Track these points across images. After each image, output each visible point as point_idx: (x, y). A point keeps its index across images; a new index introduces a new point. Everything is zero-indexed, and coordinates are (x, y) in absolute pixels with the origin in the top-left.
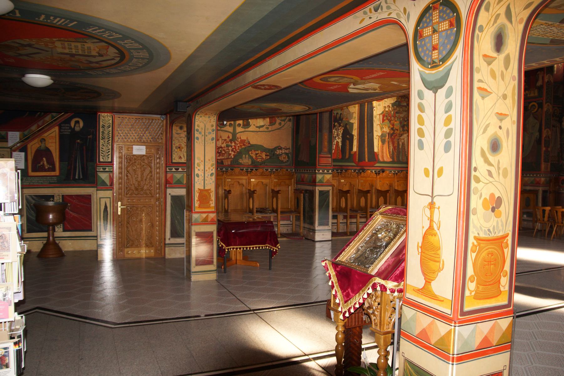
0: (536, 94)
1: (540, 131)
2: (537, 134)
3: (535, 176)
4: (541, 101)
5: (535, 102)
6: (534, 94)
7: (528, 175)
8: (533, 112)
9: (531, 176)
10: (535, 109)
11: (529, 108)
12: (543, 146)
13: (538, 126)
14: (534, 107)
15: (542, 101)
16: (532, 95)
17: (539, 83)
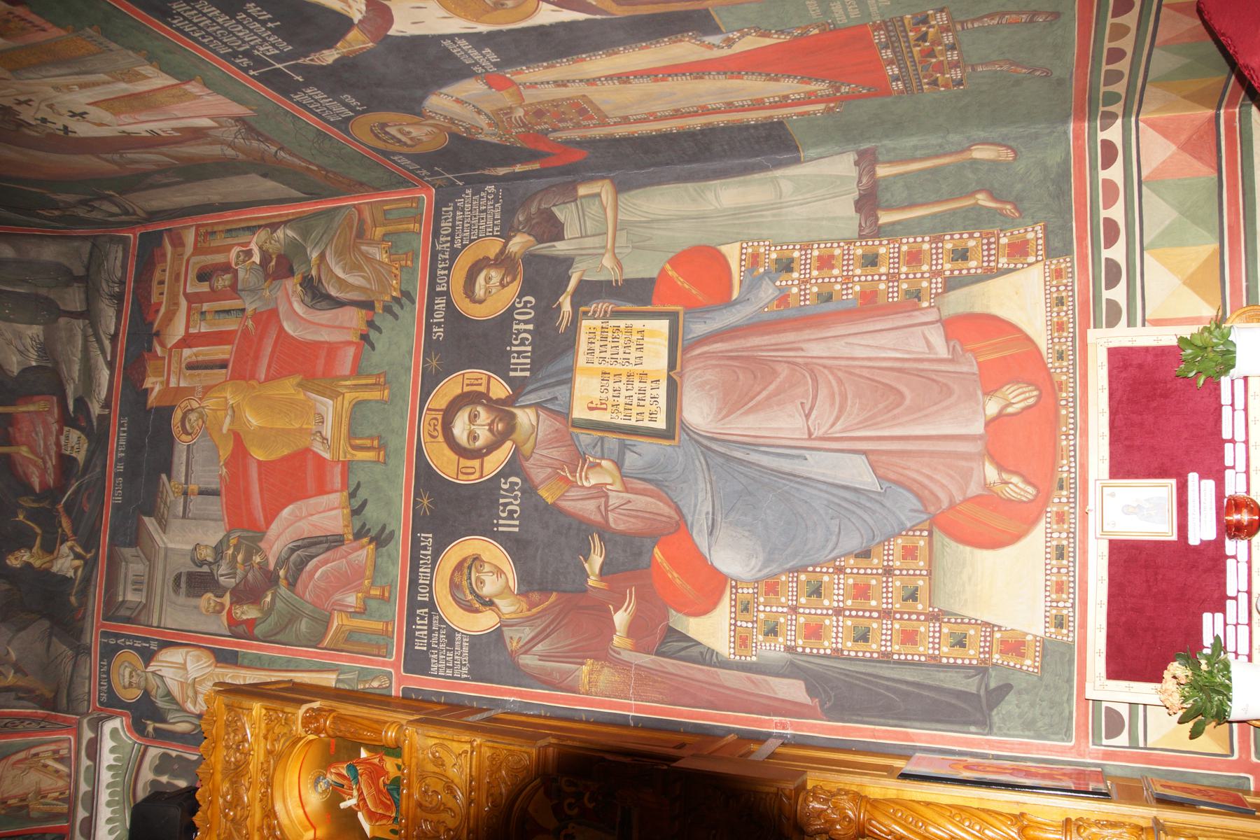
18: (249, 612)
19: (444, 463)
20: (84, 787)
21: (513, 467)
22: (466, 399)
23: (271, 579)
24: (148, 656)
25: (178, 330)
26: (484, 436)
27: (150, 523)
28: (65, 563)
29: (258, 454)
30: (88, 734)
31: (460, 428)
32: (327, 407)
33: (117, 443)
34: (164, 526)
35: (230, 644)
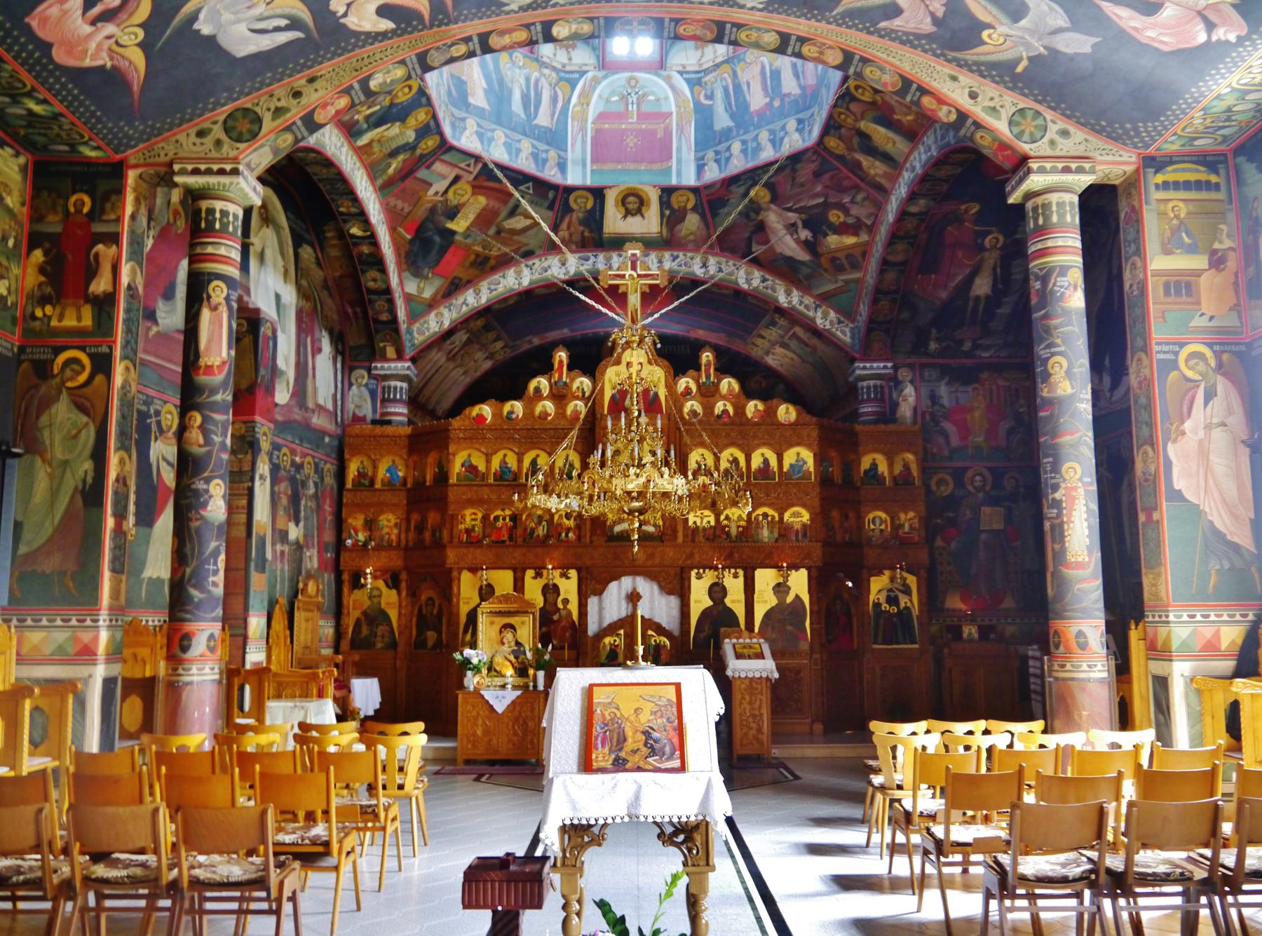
0: (87, 321)
1: (99, 456)
2: (88, 465)
3: (74, 622)
4: (105, 349)
5: (82, 349)
6: (79, 319)
7: (44, 622)
8: (69, 384)
9: (59, 622)
10: (79, 373)
11: (56, 371)
12: (109, 511)
13: (89, 436)
14: (76, 367)
15: (111, 348)
16: (70, 322)
17: (100, 285)
18: (928, 417)
19: (969, 474)
20: (875, 365)
21: (970, 493)
22: (984, 480)
23: (937, 424)
24: (912, 382)
25: (1002, 383)
26: (977, 484)
27: (947, 379)
28: (933, 346)
29: (968, 417)
30: (890, 365)
31: (978, 478)
32: (980, 439)
33: (968, 362)
34: (948, 384)
35: (919, 412)
